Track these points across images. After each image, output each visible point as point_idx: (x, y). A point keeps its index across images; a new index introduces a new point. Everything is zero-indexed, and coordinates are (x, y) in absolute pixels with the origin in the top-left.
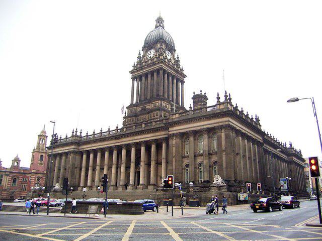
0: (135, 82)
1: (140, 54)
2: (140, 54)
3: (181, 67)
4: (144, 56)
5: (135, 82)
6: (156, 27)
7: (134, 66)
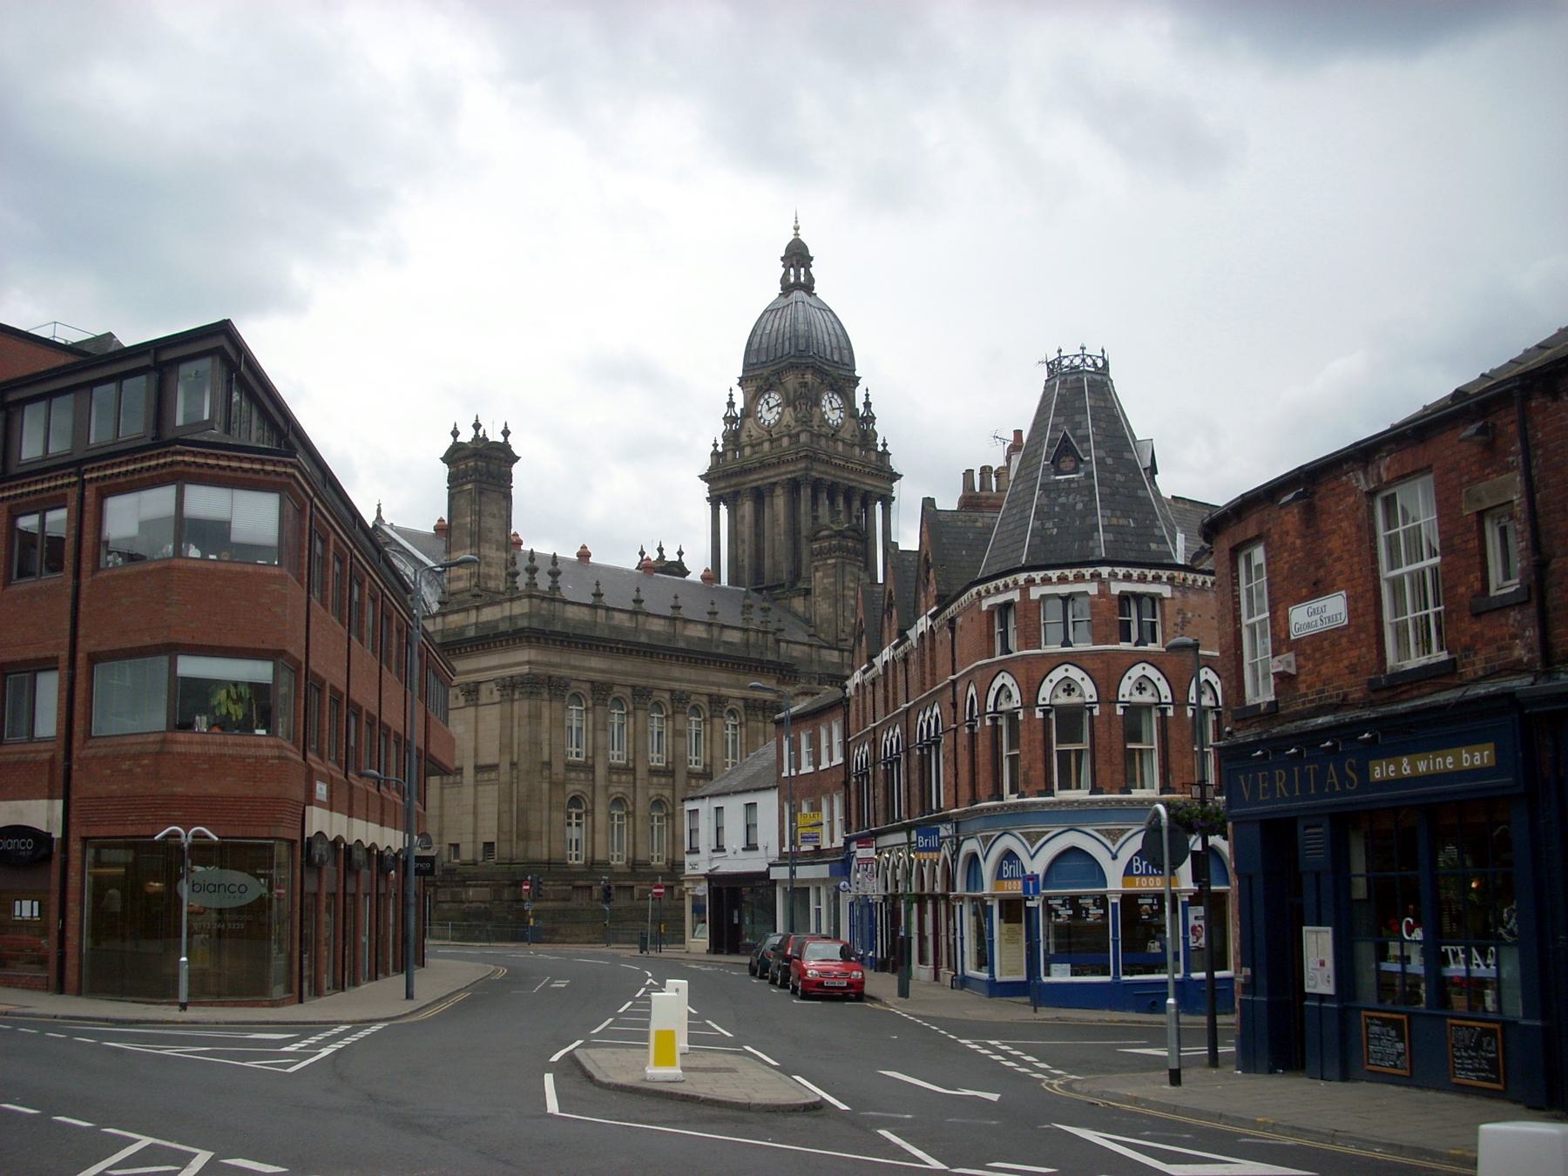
0: (723, 510)
1: (731, 404)
2: (731, 404)
3: (879, 441)
4: (748, 412)
5: (723, 510)
6: (787, 288)
7: (715, 454)
